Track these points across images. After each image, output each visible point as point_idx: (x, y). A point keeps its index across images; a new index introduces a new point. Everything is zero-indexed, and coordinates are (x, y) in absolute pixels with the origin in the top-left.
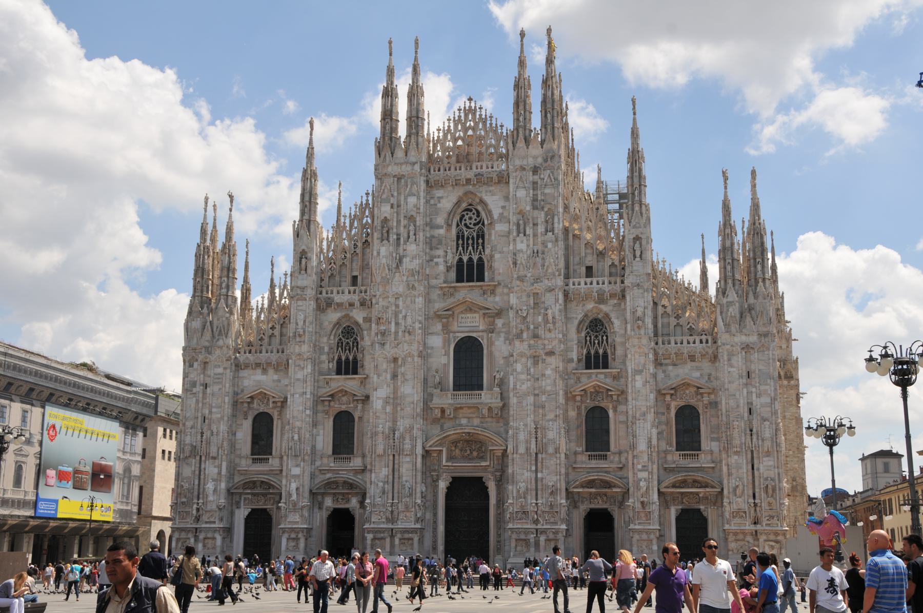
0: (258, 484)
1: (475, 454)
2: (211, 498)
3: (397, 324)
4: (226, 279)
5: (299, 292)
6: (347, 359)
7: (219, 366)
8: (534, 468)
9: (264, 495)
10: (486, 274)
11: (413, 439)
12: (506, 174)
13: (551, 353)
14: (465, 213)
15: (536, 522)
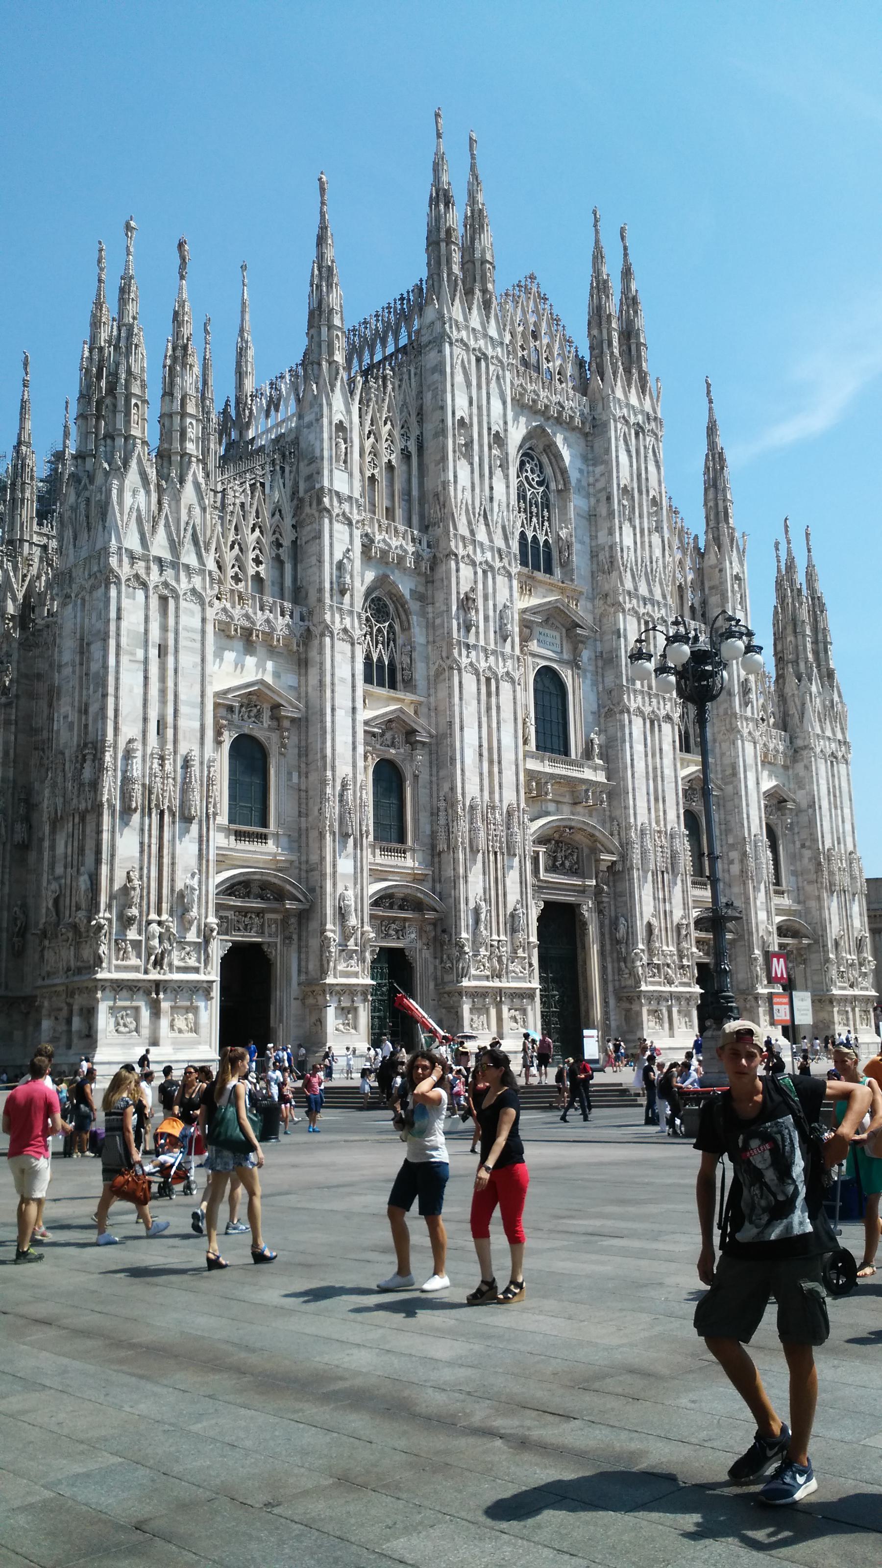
0: (256, 890)
1: (567, 864)
2: (194, 913)
3: (486, 618)
4: (194, 422)
5: (336, 503)
6: (380, 659)
7: (192, 613)
8: (661, 896)
9: (260, 913)
10: (558, 571)
11: (523, 826)
12: (590, 418)
13: (668, 718)
14: (526, 459)
15: (670, 982)
